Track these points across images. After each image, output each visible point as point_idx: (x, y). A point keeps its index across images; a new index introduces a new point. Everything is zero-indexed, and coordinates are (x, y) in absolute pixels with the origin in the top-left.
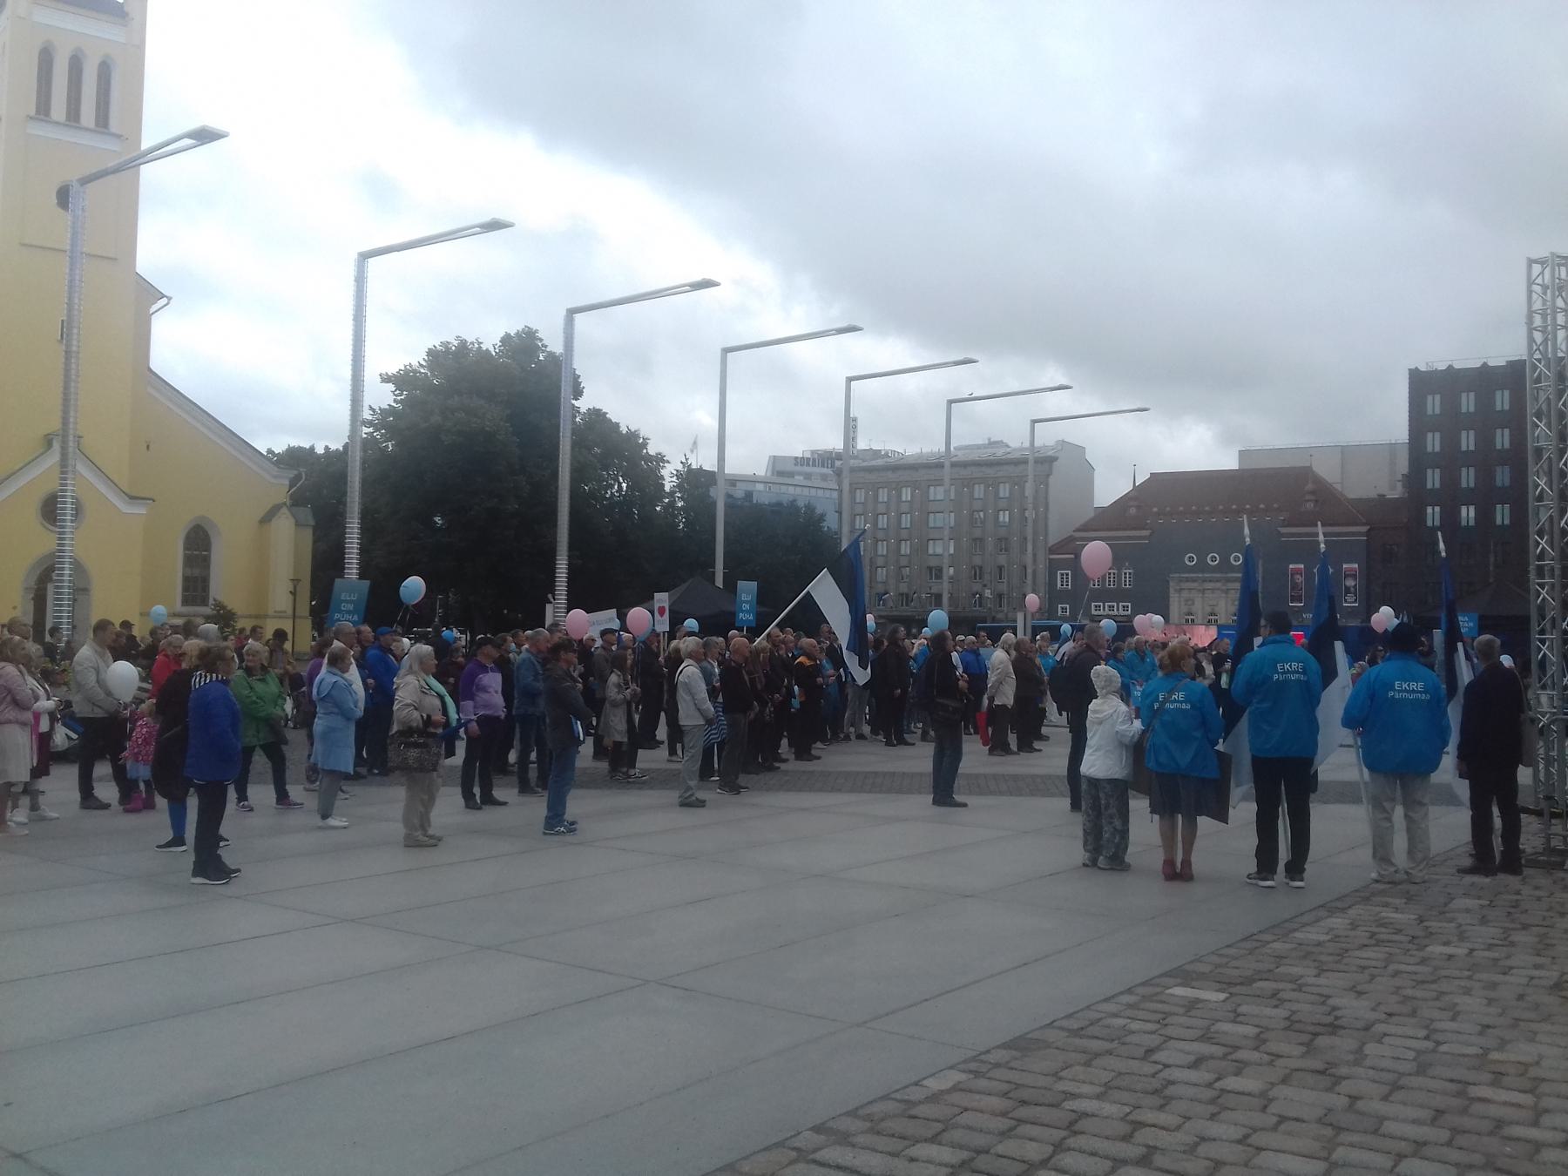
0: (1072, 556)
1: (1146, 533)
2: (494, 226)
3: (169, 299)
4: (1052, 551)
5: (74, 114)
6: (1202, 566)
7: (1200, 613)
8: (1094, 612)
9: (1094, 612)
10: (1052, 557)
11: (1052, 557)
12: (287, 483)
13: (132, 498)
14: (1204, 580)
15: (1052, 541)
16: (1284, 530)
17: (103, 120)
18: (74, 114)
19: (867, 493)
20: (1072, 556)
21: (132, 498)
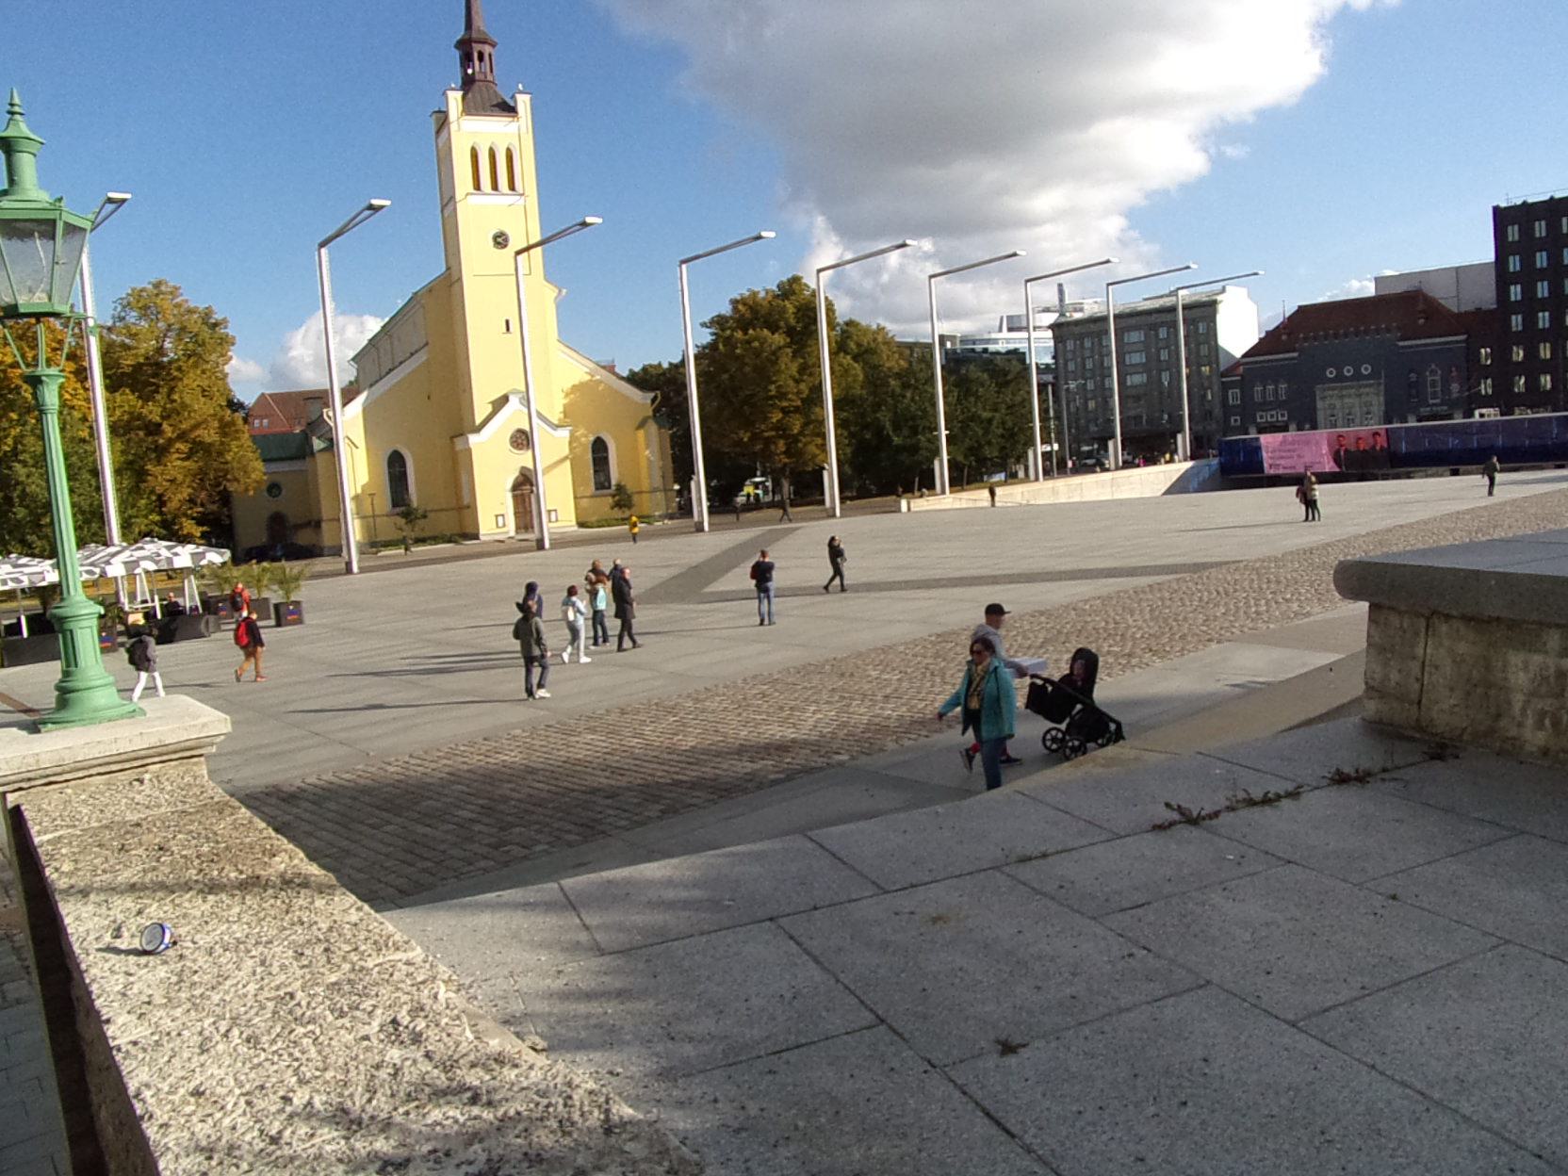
0: (1239, 378)
1: (1295, 355)
2: (508, 329)
4: (1223, 375)
5: (495, 187)
6: (1340, 378)
7: (1340, 415)
8: (1259, 420)
9: (1259, 420)
10: (1224, 380)
11: (1224, 380)
14: (1342, 388)
15: (1222, 369)
16: (1401, 344)
17: (512, 187)
18: (495, 187)
19: (1075, 344)
20: (1239, 378)
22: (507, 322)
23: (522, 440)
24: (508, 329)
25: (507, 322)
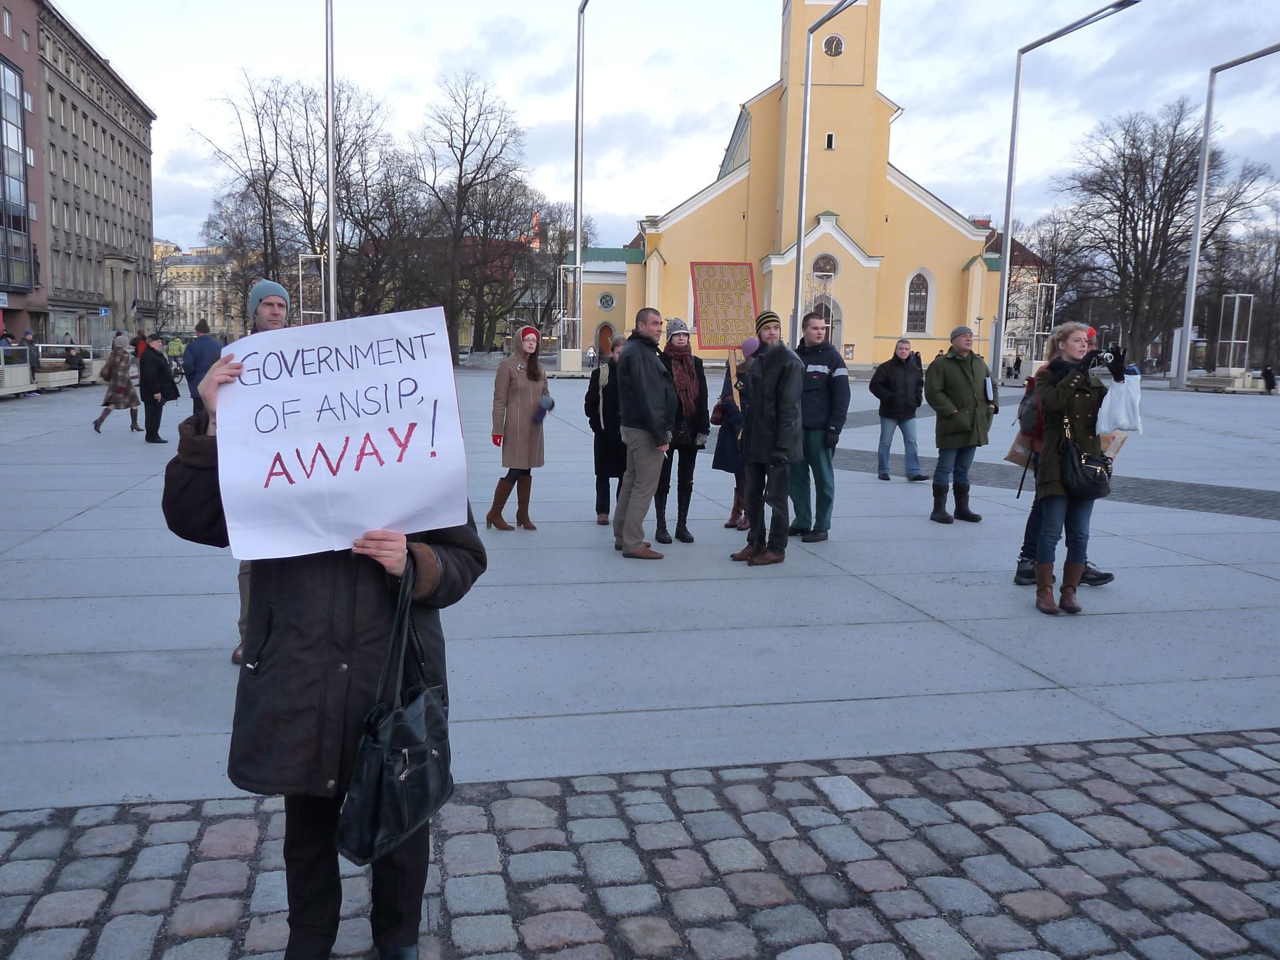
3: (903, 110)
12: (984, 239)
13: (869, 257)
21: (869, 257)
22: (830, 137)
24: (830, 145)
25: (830, 137)
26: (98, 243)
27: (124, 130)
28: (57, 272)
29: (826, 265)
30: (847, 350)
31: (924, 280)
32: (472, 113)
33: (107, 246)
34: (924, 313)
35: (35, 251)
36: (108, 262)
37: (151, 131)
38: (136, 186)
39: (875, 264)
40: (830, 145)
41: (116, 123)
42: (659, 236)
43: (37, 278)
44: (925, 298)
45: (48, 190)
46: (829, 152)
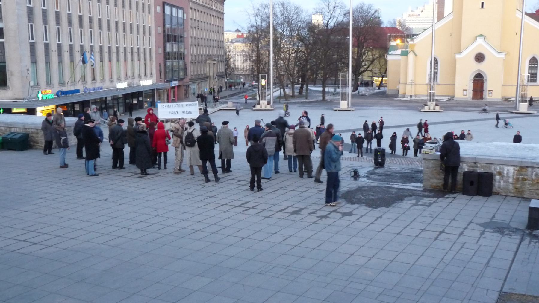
22: (483, 3)
23: (480, 58)
24: (482, 6)
25: (483, 3)
26: (205, 55)
27: (215, 10)
28: (192, 69)
29: (480, 58)
30: (490, 92)
31: (536, 59)
32: (331, 8)
33: (208, 55)
34: (536, 74)
35: (186, 65)
36: (208, 62)
37: (225, 5)
38: (218, 29)
39: (502, 56)
40: (482, 6)
41: (212, 9)
42: (414, 45)
43: (186, 73)
44: (537, 67)
45: (190, 43)
46: (482, 9)
